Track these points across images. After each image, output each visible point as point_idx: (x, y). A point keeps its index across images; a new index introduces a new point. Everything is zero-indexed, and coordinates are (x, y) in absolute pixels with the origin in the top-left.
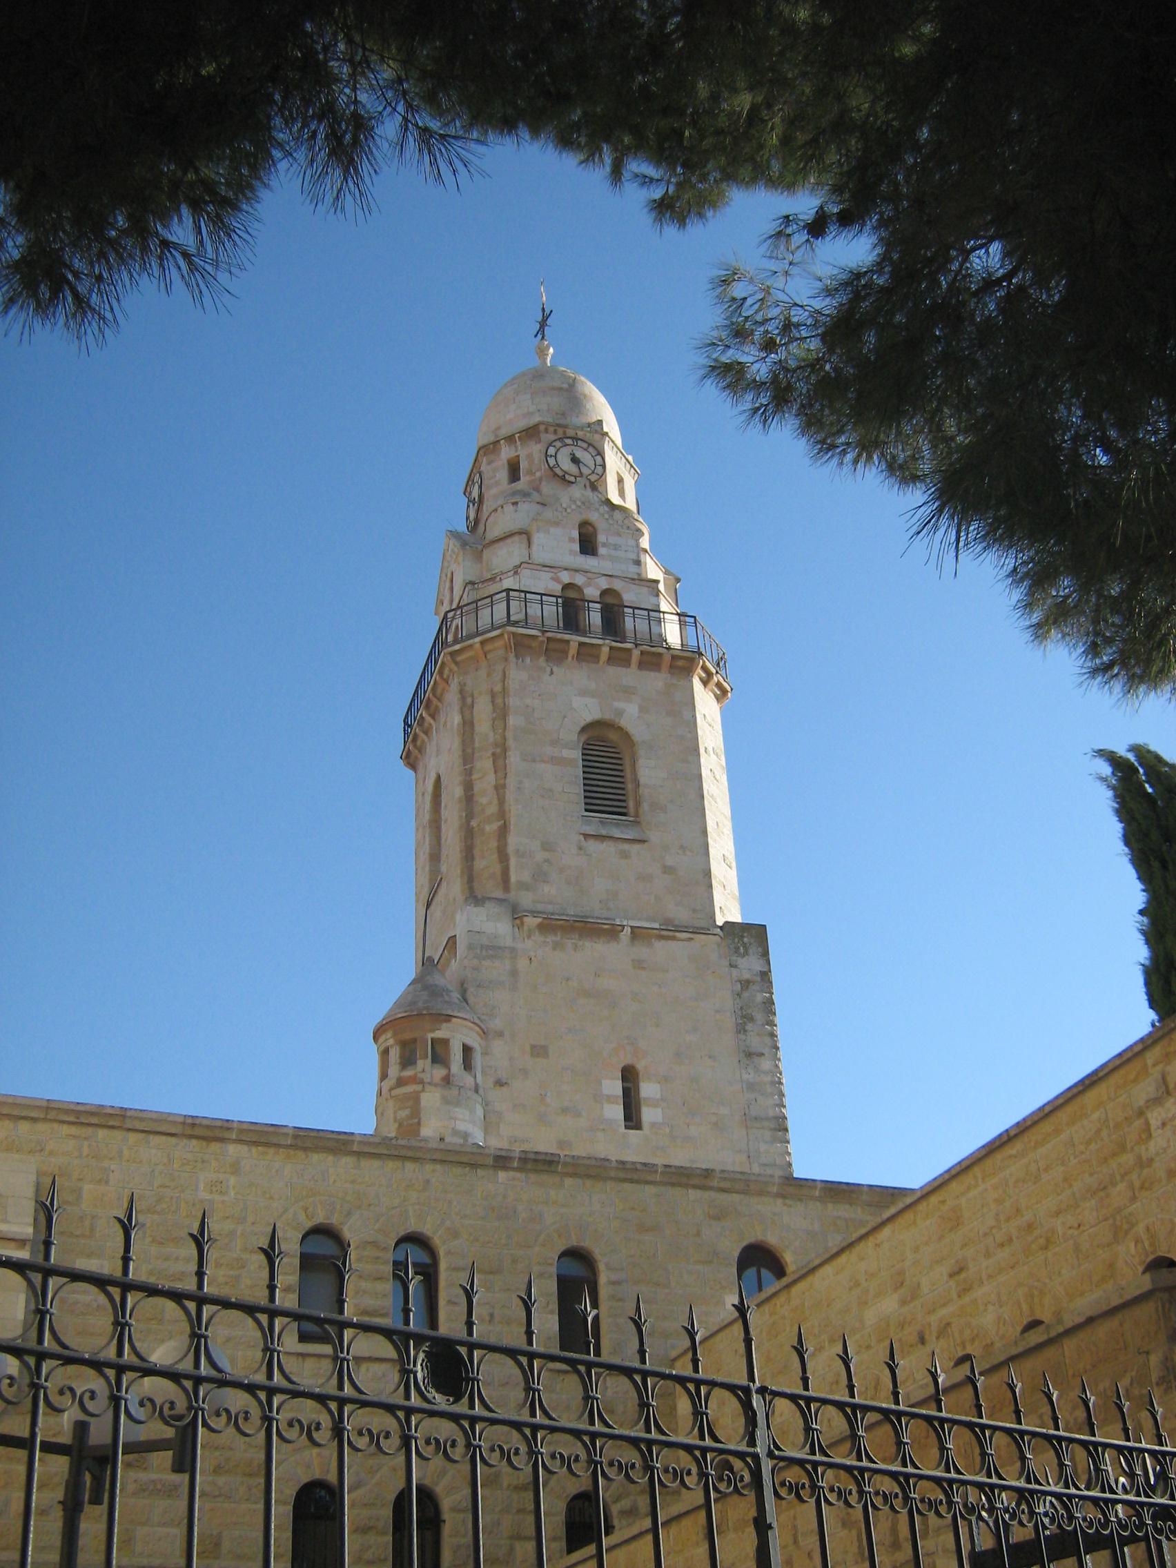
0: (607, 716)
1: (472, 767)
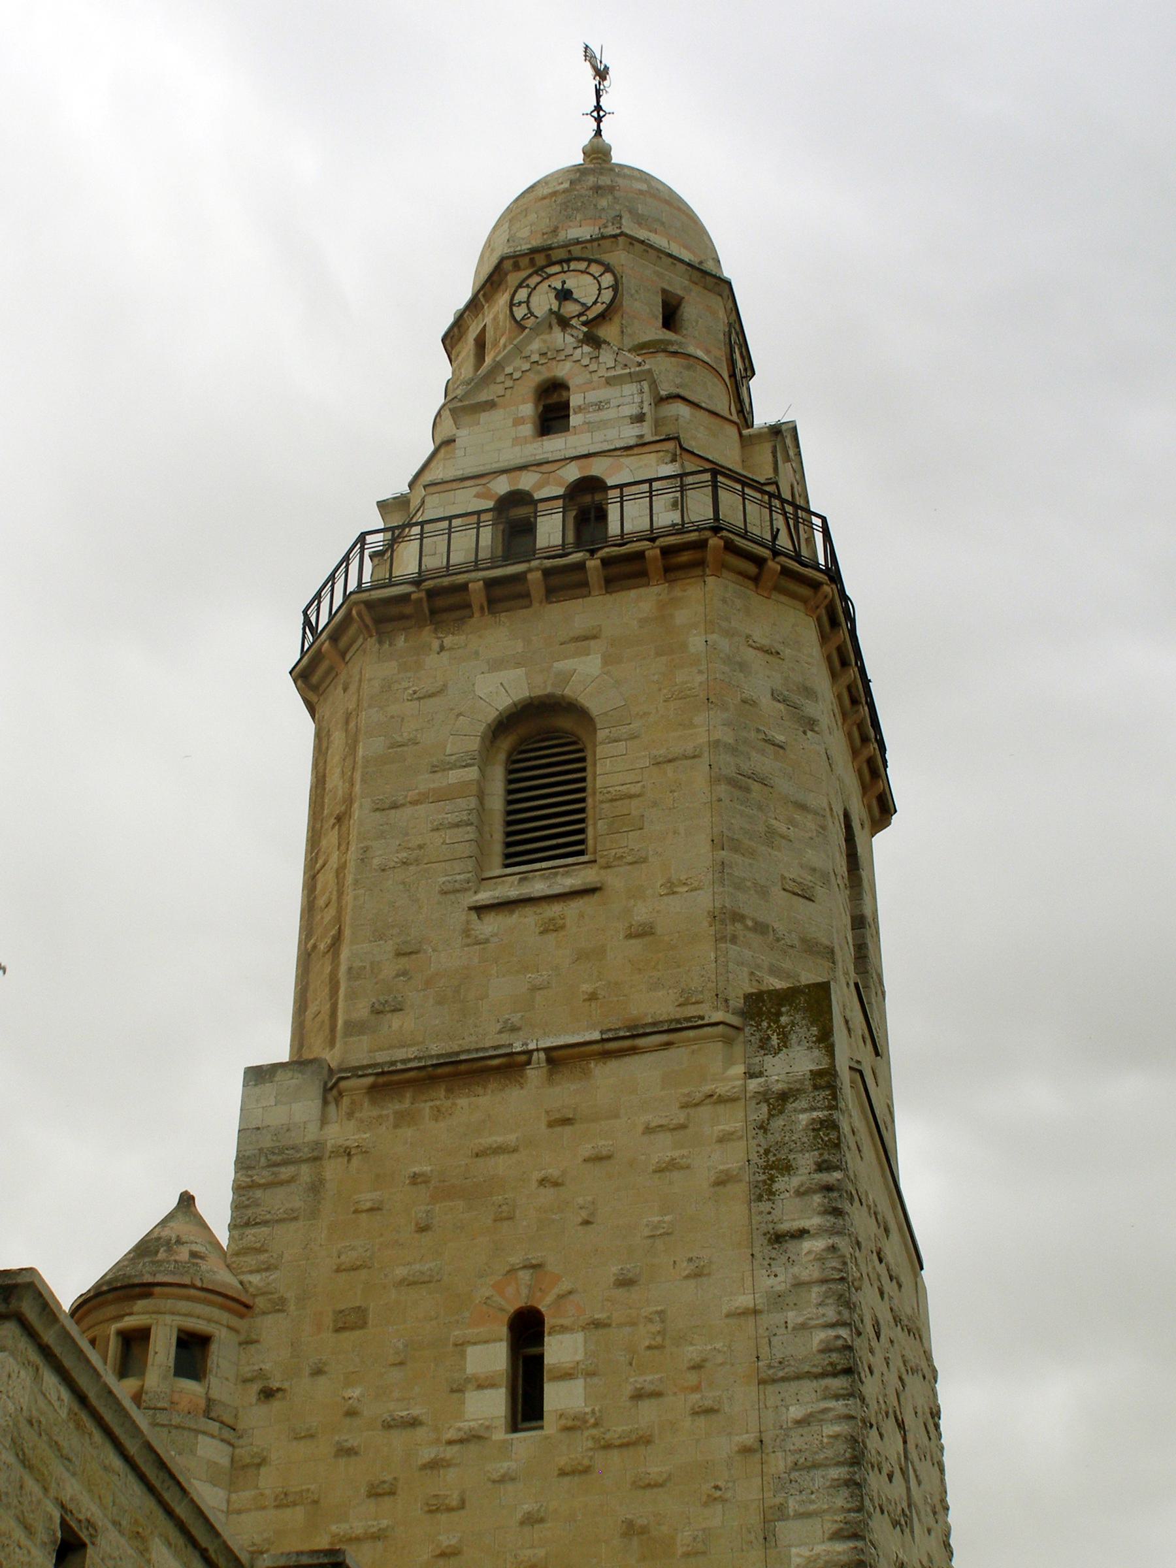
0: (542, 686)
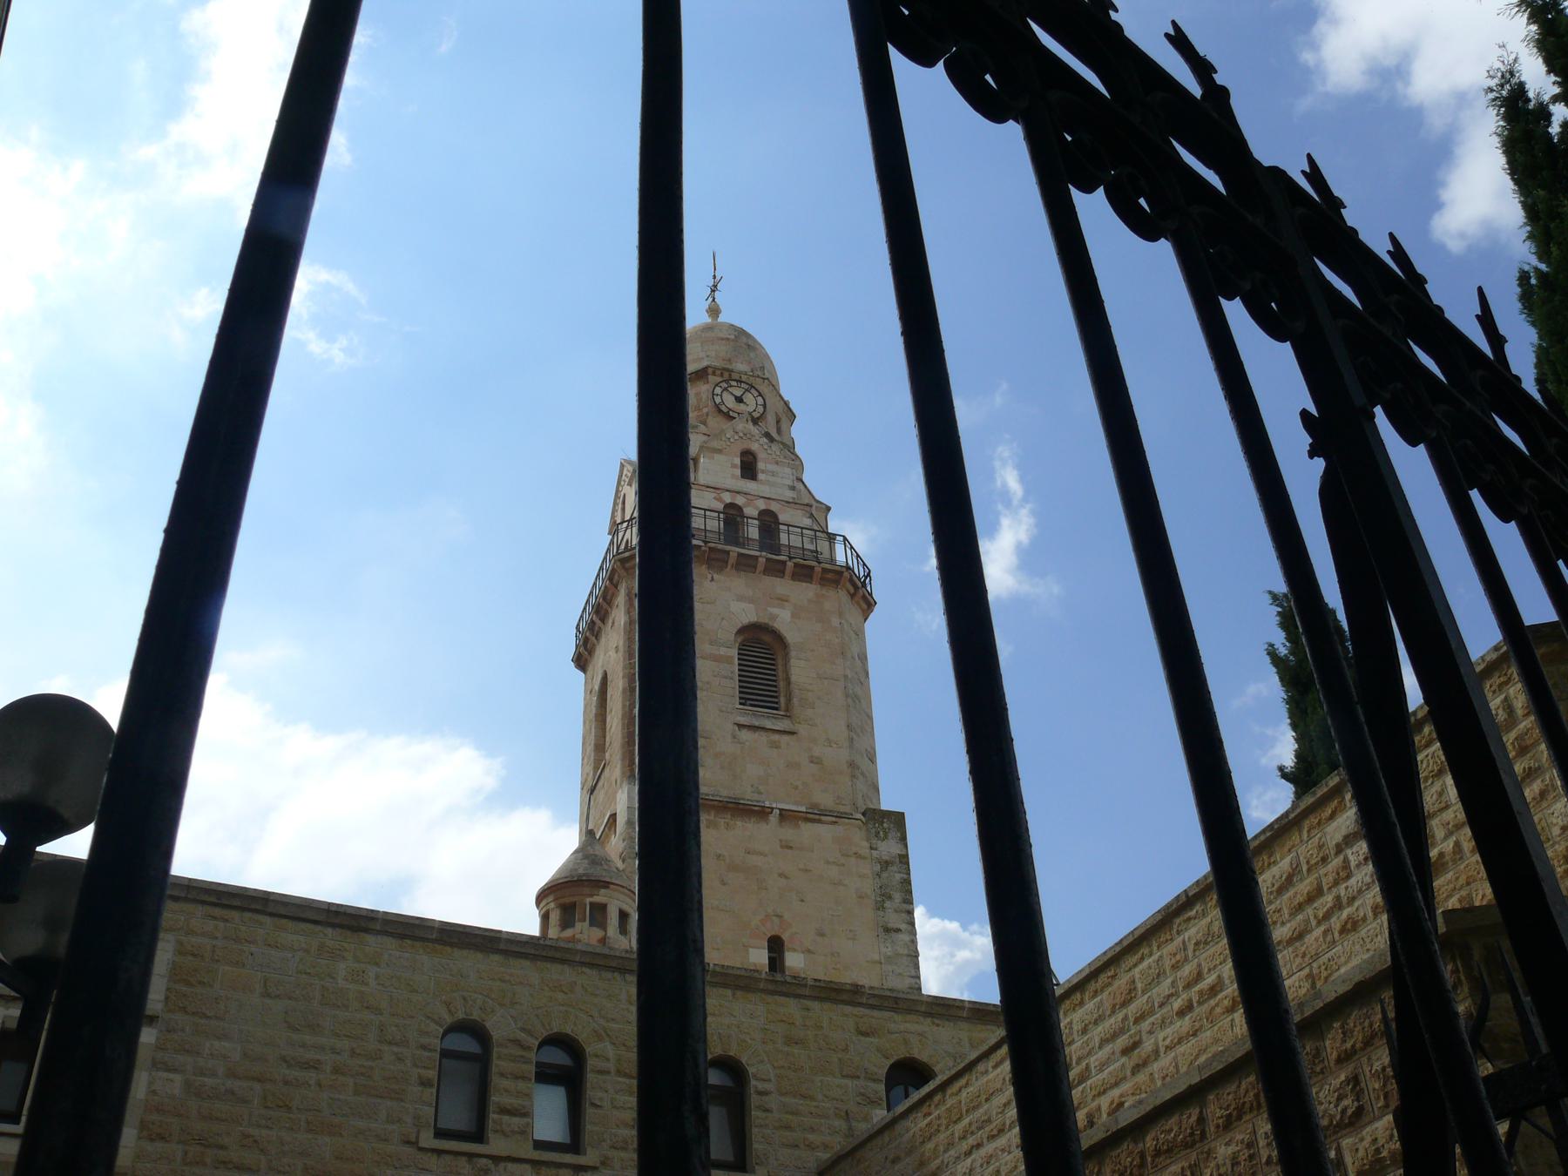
0: (764, 620)
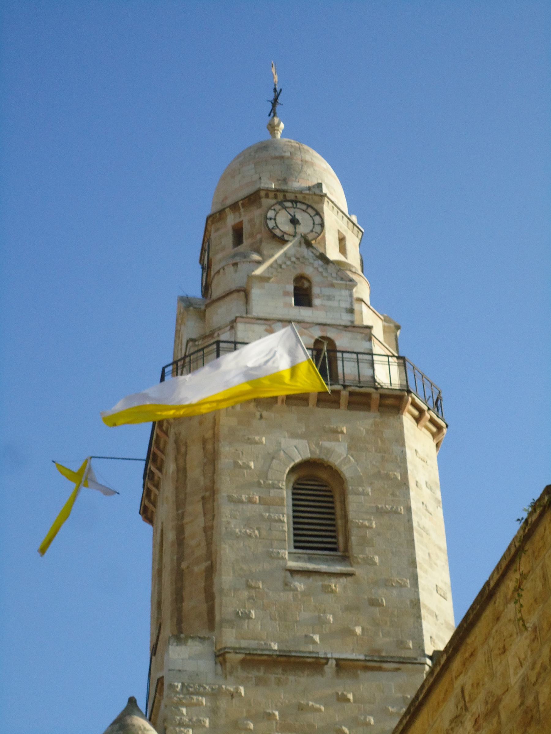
0: (318, 454)
1: (183, 513)
